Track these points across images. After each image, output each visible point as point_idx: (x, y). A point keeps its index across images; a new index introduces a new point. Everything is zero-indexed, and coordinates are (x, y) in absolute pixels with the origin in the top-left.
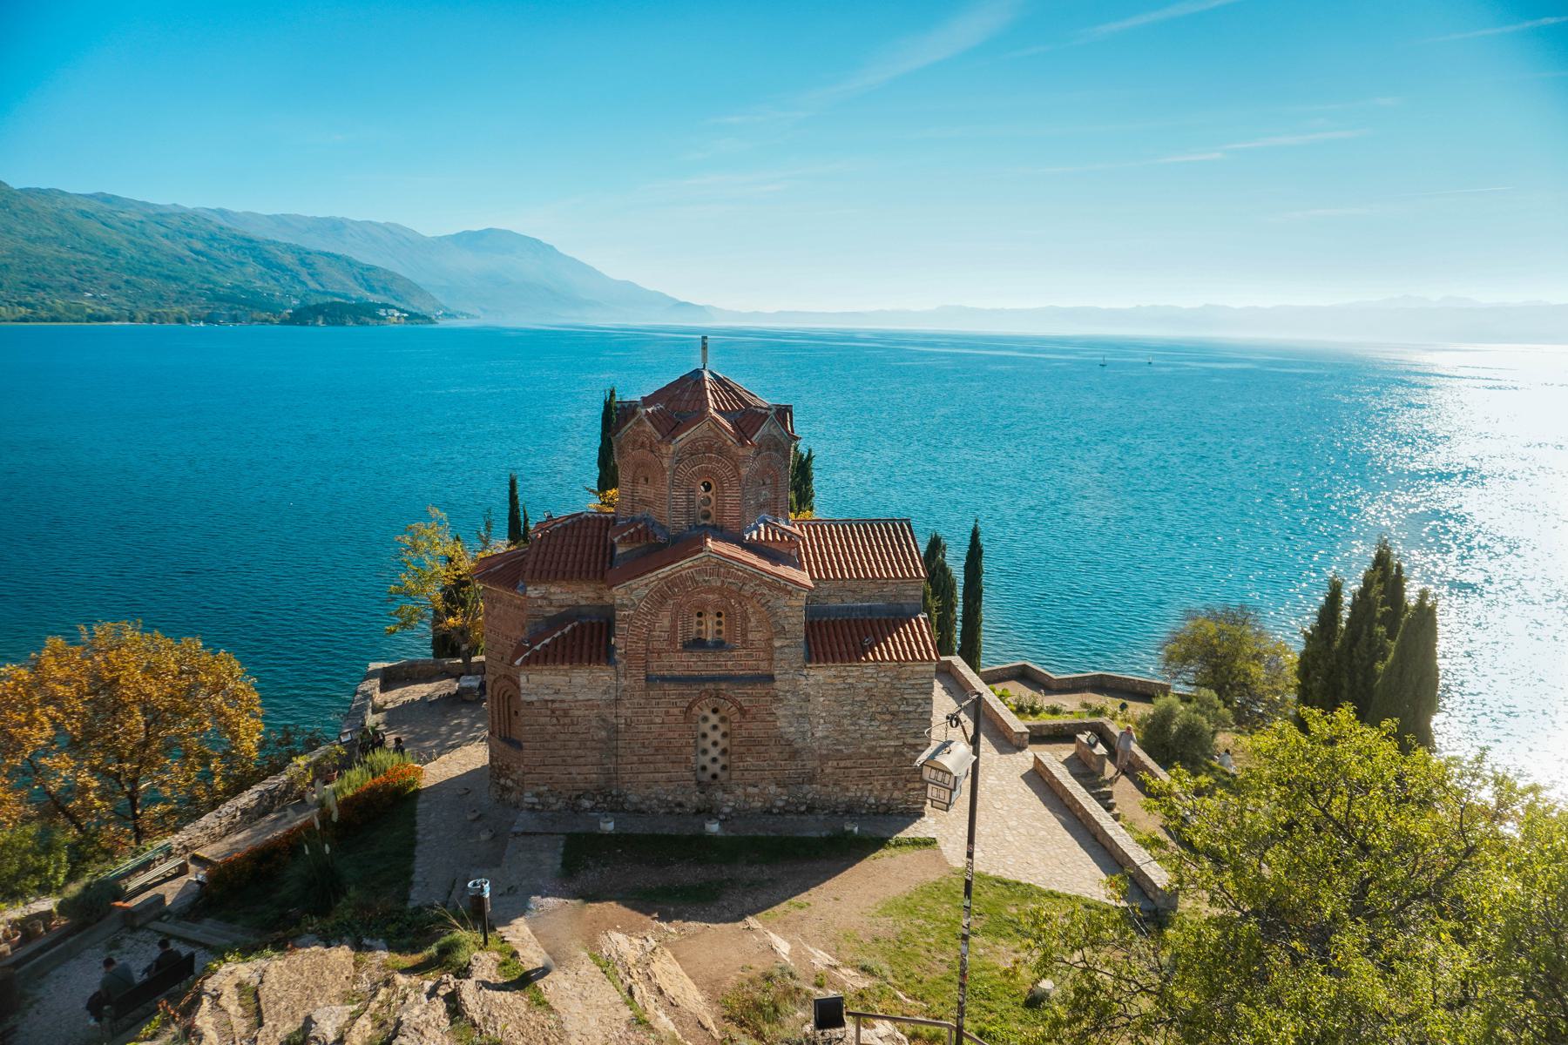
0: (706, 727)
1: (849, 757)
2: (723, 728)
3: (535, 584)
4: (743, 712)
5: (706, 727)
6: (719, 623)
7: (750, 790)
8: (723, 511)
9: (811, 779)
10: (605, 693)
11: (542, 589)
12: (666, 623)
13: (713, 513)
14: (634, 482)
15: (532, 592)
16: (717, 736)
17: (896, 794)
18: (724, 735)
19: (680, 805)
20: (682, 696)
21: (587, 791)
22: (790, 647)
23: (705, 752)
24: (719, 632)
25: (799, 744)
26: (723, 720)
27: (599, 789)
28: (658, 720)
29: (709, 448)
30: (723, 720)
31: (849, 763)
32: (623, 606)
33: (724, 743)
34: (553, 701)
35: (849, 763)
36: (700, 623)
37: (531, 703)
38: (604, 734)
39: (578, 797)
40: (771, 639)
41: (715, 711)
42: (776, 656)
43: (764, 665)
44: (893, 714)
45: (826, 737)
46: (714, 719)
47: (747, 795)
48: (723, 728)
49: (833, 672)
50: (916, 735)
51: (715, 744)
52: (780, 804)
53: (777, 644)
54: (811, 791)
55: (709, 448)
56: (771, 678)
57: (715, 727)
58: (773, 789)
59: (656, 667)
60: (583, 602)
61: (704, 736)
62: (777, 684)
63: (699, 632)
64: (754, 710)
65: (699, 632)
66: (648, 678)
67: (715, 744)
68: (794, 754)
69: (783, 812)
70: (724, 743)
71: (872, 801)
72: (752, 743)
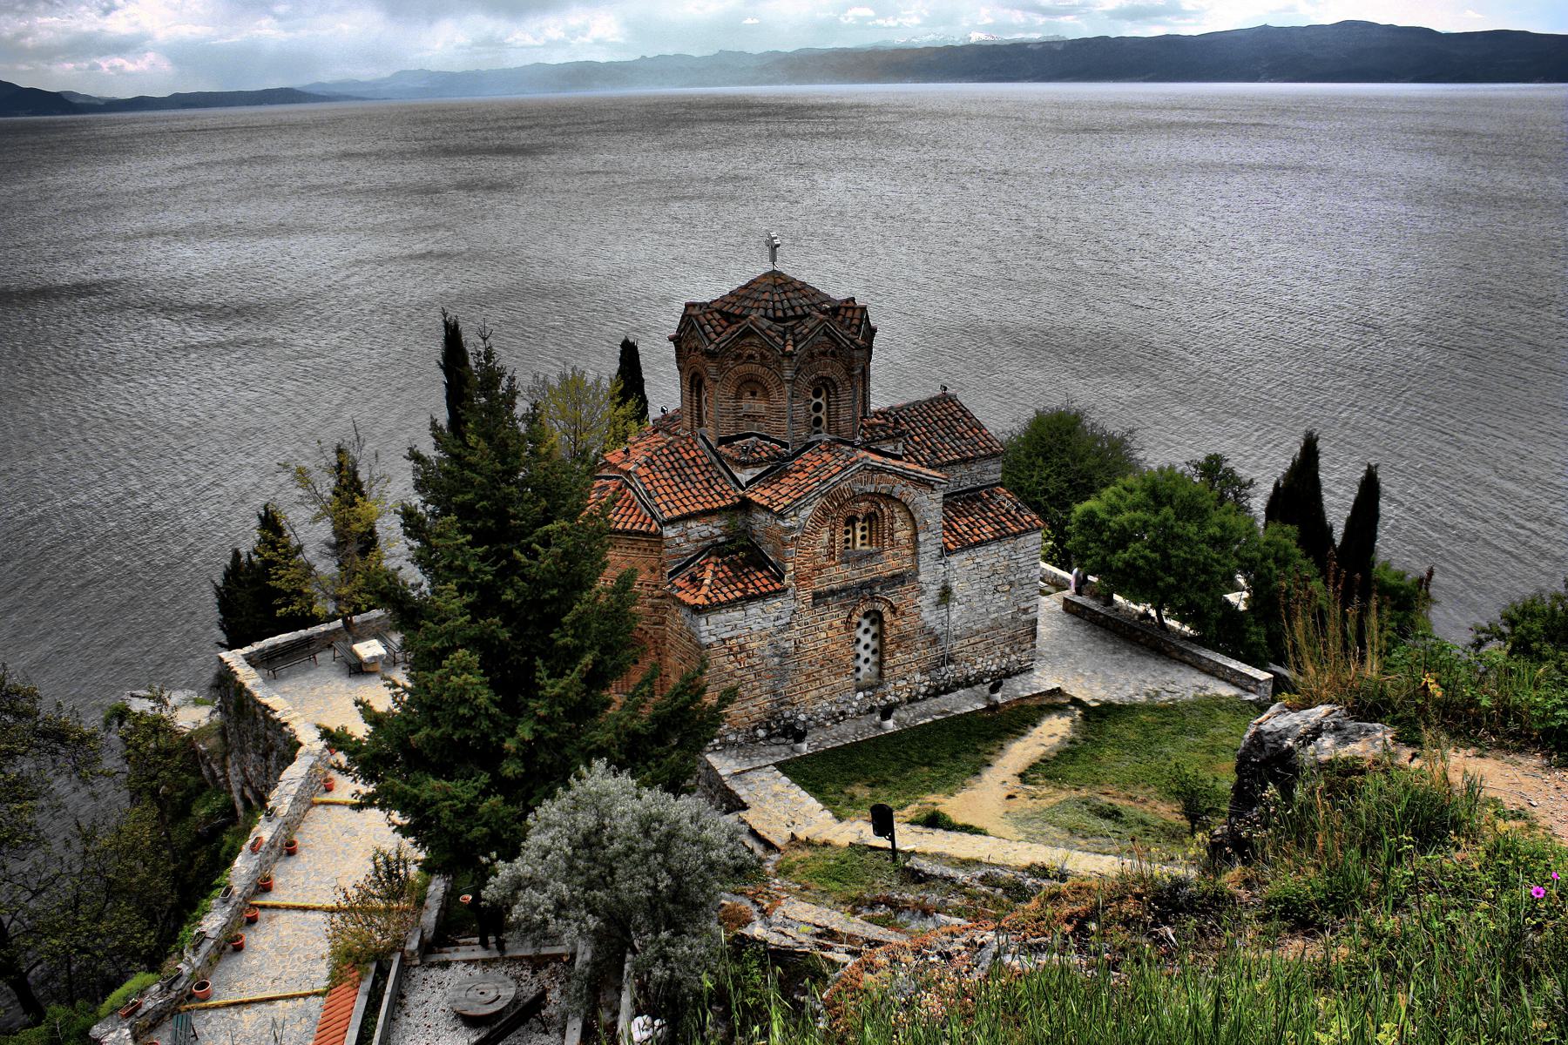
0: (859, 633)
1: (978, 632)
2: (873, 630)
3: (672, 522)
4: (894, 610)
5: (859, 633)
6: (863, 529)
7: (901, 683)
8: (837, 414)
9: (951, 660)
10: (778, 618)
11: (680, 527)
12: (826, 536)
13: (824, 418)
14: (738, 397)
15: (669, 532)
16: (867, 639)
17: (1013, 657)
18: (874, 637)
19: (843, 713)
20: (843, 606)
21: (761, 721)
22: (930, 544)
23: (858, 656)
24: (863, 537)
25: (939, 629)
26: (873, 623)
27: (771, 718)
28: (823, 635)
29: (824, 354)
30: (873, 623)
31: (977, 639)
32: (792, 529)
33: (874, 644)
34: (730, 639)
35: (977, 639)
36: (847, 532)
37: (709, 646)
38: (776, 660)
39: (755, 729)
40: (916, 534)
41: (866, 615)
42: (921, 549)
43: (907, 564)
44: (1011, 584)
45: (960, 618)
46: (866, 624)
47: (896, 689)
48: (873, 630)
49: (965, 555)
50: (1028, 600)
51: (866, 647)
52: (923, 690)
53: (921, 538)
54: (950, 672)
55: (824, 354)
56: (918, 573)
57: (866, 631)
58: (918, 677)
59: (819, 585)
60: (717, 532)
61: (858, 641)
62: (921, 578)
63: (847, 541)
64: (902, 608)
65: (847, 541)
66: (818, 598)
67: (866, 647)
68: (936, 641)
69: (926, 696)
70: (874, 644)
71: (994, 668)
72: (902, 638)
